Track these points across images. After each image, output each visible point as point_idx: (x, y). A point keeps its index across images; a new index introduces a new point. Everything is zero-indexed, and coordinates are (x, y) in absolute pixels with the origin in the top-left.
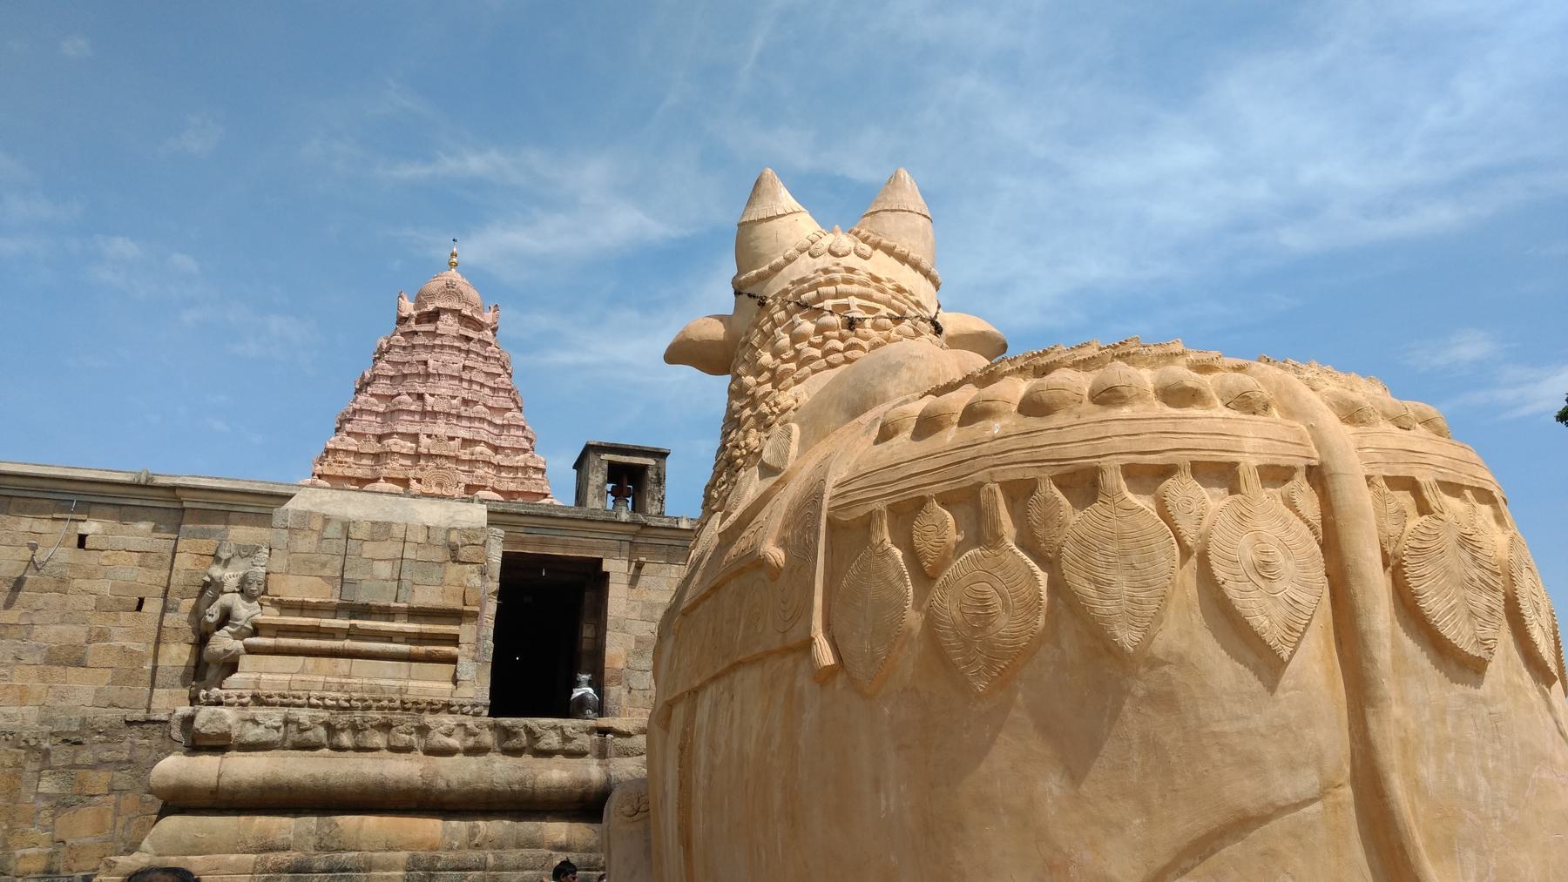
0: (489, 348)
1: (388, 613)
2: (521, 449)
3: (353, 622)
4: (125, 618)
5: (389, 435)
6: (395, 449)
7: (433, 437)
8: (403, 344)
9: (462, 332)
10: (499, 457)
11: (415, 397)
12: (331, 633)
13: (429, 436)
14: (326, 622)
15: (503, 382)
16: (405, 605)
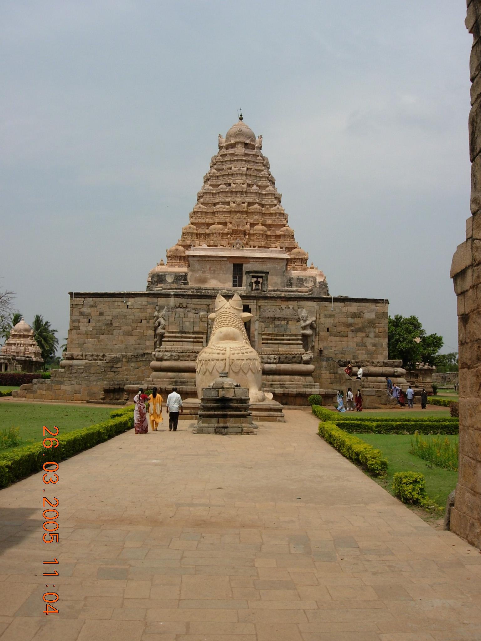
0: (258, 158)
1: (189, 333)
2: (274, 204)
3: (182, 335)
4: (139, 324)
5: (218, 203)
6: (221, 210)
7: (236, 203)
8: (222, 160)
9: (246, 152)
10: (263, 209)
11: (228, 185)
12: (178, 337)
13: (234, 203)
14: (177, 335)
15: (265, 174)
16: (192, 331)
